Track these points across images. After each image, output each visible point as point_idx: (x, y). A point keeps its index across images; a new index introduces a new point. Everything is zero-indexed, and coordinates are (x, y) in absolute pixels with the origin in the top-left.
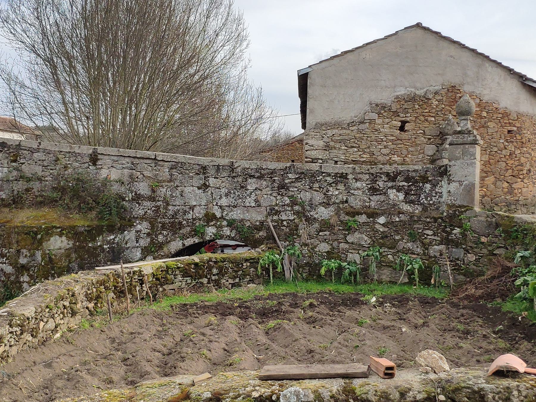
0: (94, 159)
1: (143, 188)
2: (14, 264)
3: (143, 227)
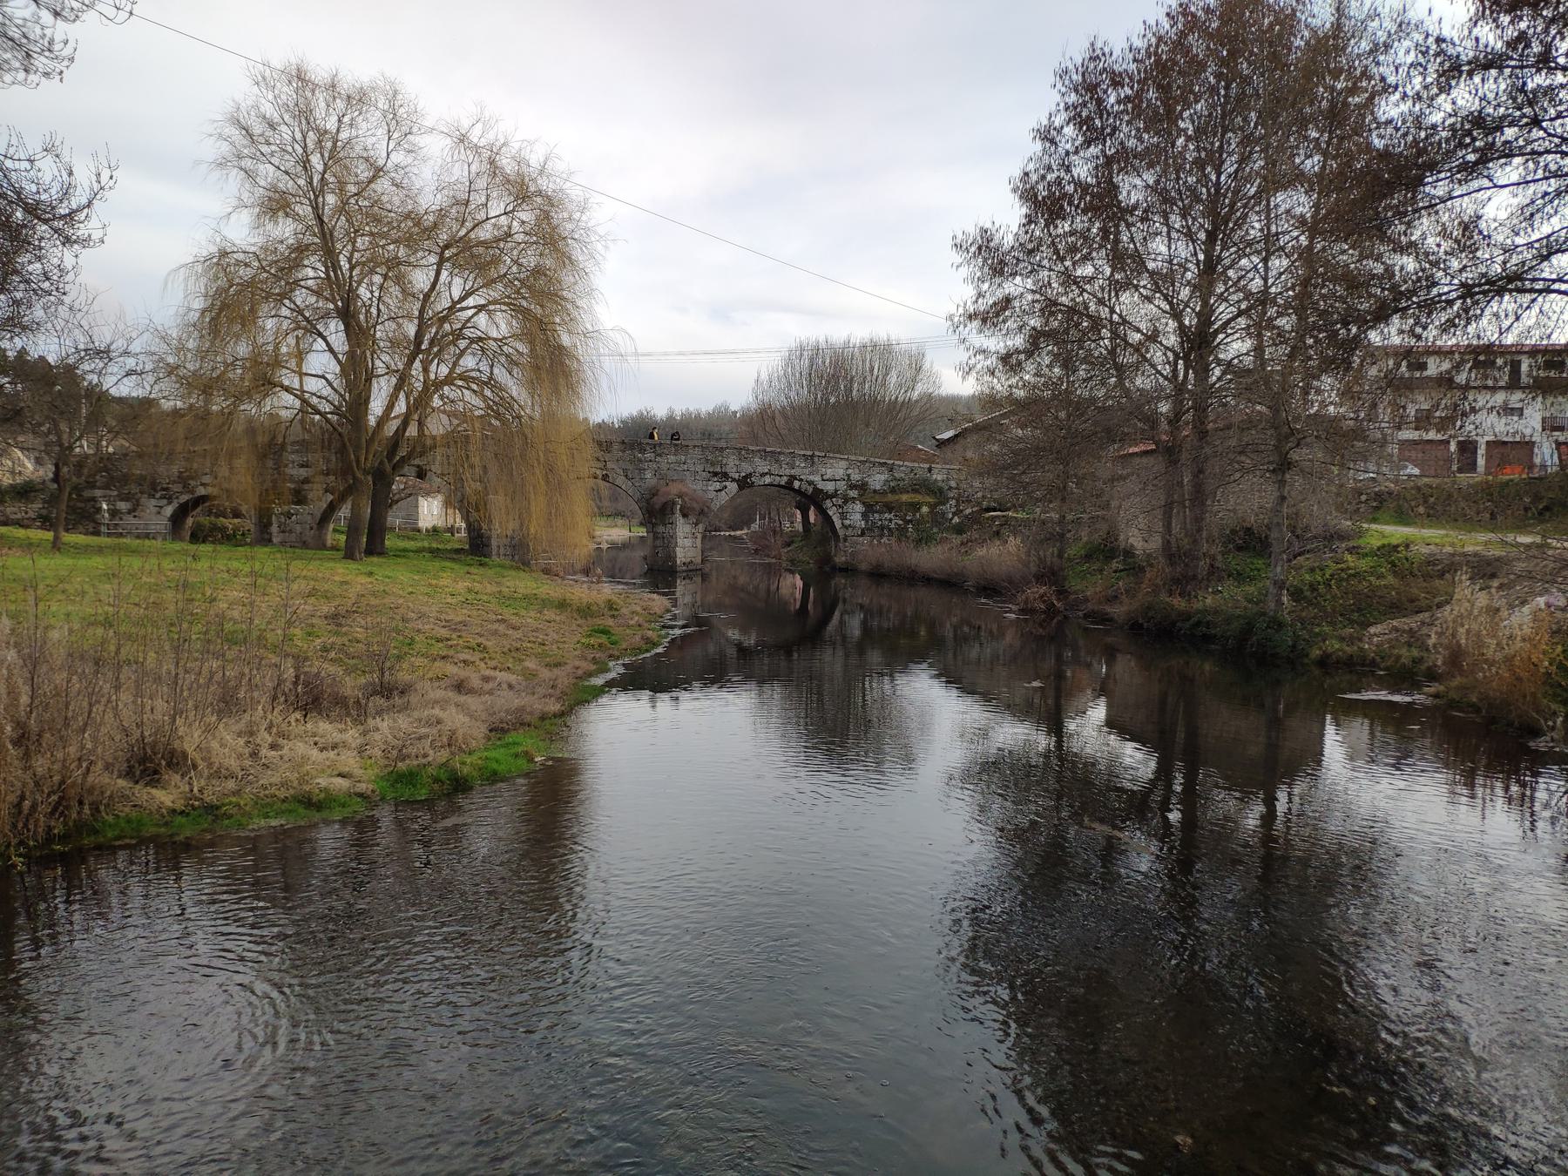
0: (930, 470)
1: (953, 484)
3: (953, 502)
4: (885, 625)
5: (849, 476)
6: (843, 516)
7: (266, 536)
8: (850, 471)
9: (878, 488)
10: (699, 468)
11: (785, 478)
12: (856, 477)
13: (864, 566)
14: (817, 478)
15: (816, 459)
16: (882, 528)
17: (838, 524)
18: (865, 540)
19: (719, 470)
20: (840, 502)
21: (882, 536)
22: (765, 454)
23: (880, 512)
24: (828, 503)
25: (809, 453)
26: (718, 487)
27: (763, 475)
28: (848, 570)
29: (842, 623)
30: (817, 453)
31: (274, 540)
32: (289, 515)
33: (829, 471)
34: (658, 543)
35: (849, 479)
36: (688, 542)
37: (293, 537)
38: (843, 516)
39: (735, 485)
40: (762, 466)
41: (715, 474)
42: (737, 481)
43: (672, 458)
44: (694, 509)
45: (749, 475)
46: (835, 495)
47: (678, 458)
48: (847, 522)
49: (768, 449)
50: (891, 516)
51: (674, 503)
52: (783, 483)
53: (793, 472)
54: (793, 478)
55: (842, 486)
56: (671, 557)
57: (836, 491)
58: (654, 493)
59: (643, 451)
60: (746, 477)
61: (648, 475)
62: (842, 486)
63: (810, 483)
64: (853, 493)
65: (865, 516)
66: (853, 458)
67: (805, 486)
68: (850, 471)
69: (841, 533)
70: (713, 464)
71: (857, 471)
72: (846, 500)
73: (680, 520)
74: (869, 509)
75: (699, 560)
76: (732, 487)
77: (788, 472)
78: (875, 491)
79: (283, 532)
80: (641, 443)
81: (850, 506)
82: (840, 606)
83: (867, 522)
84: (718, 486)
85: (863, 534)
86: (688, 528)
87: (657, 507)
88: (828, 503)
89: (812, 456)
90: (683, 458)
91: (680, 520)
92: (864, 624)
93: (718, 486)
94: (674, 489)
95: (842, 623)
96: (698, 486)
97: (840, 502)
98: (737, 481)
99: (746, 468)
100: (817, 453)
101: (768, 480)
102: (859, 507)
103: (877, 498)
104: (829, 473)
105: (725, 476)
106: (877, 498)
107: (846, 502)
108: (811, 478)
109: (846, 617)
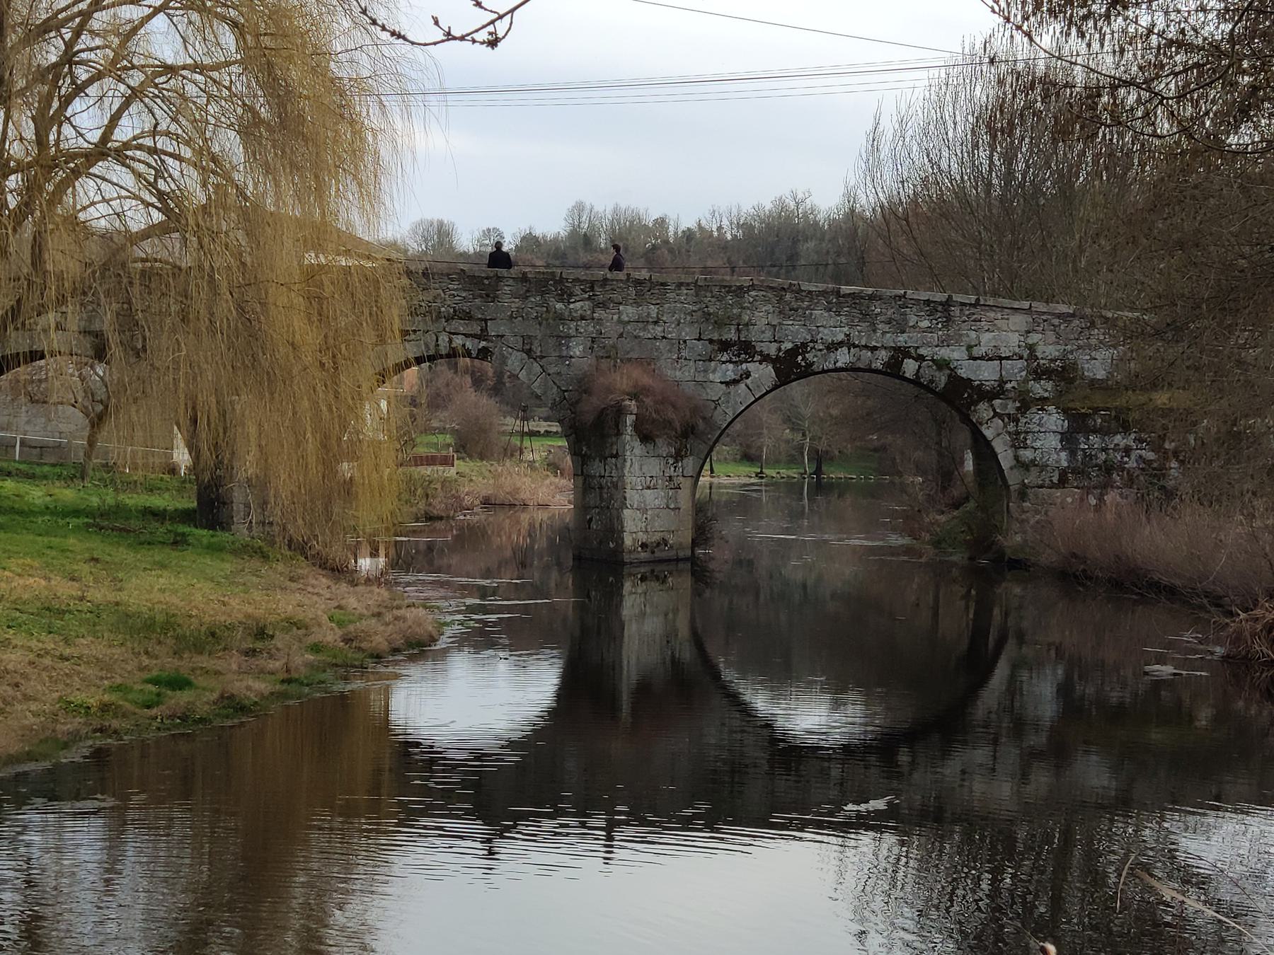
2: (1157, 447)
4: (1114, 696)
5: (1031, 348)
6: (1018, 441)
8: (1034, 338)
9: (1101, 375)
10: (688, 333)
11: (884, 355)
12: (1048, 350)
13: (1047, 558)
14: (955, 354)
15: (955, 311)
16: (1108, 468)
17: (1006, 461)
18: (1069, 496)
19: (731, 335)
20: (1011, 407)
21: (1106, 486)
22: (836, 302)
23: (1104, 432)
24: (983, 411)
25: (940, 297)
26: (730, 375)
27: (833, 347)
28: (1017, 566)
29: (1013, 688)
30: (958, 298)
33: (986, 337)
34: (593, 499)
35: (1033, 356)
36: (654, 498)
38: (1018, 441)
39: (768, 370)
40: (831, 327)
41: (725, 346)
42: (774, 361)
43: (629, 312)
44: (668, 424)
45: (801, 348)
46: (999, 391)
47: (643, 310)
48: (1027, 455)
49: (846, 289)
50: (1130, 441)
51: (620, 411)
52: (878, 365)
53: (902, 339)
54: (901, 353)
55: (1015, 370)
56: (614, 530)
57: (1002, 382)
58: (584, 386)
59: (565, 296)
60: (794, 352)
61: (577, 350)
62: (1015, 370)
63: (942, 365)
64: (1041, 388)
65: (1068, 440)
66: (1040, 306)
67: (928, 372)
68: (1034, 338)
69: (1013, 478)
70: (719, 324)
71: (1051, 336)
72: (1026, 403)
73: (633, 448)
74: (1078, 425)
75: (686, 536)
76: (763, 373)
77: (889, 340)
78: (1093, 383)
80: (562, 280)
81: (1034, 416)
82: (1010, 649)
83: (1073, 453)
84: (730, 371)
85: (1063, 482)
86: (654, 467)
87: (590, 418)
88: (983, 411)
89: (948, 304)
90: (654, 310)
91: (633, 448)
92: (1065, 691)
93: (730, 371)
94: (622, 379)
95: (1013, 688)
96: (683, 374)
97: (1011, 407)
98: (774, 361)
99: (795, 332)
100: (958, 298)
101: (843, 357)
102: (1054, 420)
103: (1098, 399)
104: (987, 341)
105: (746, 349)
106: (1098, 399)
107: (1024, 407)
108: (944, 353)
109: (1024, 675)
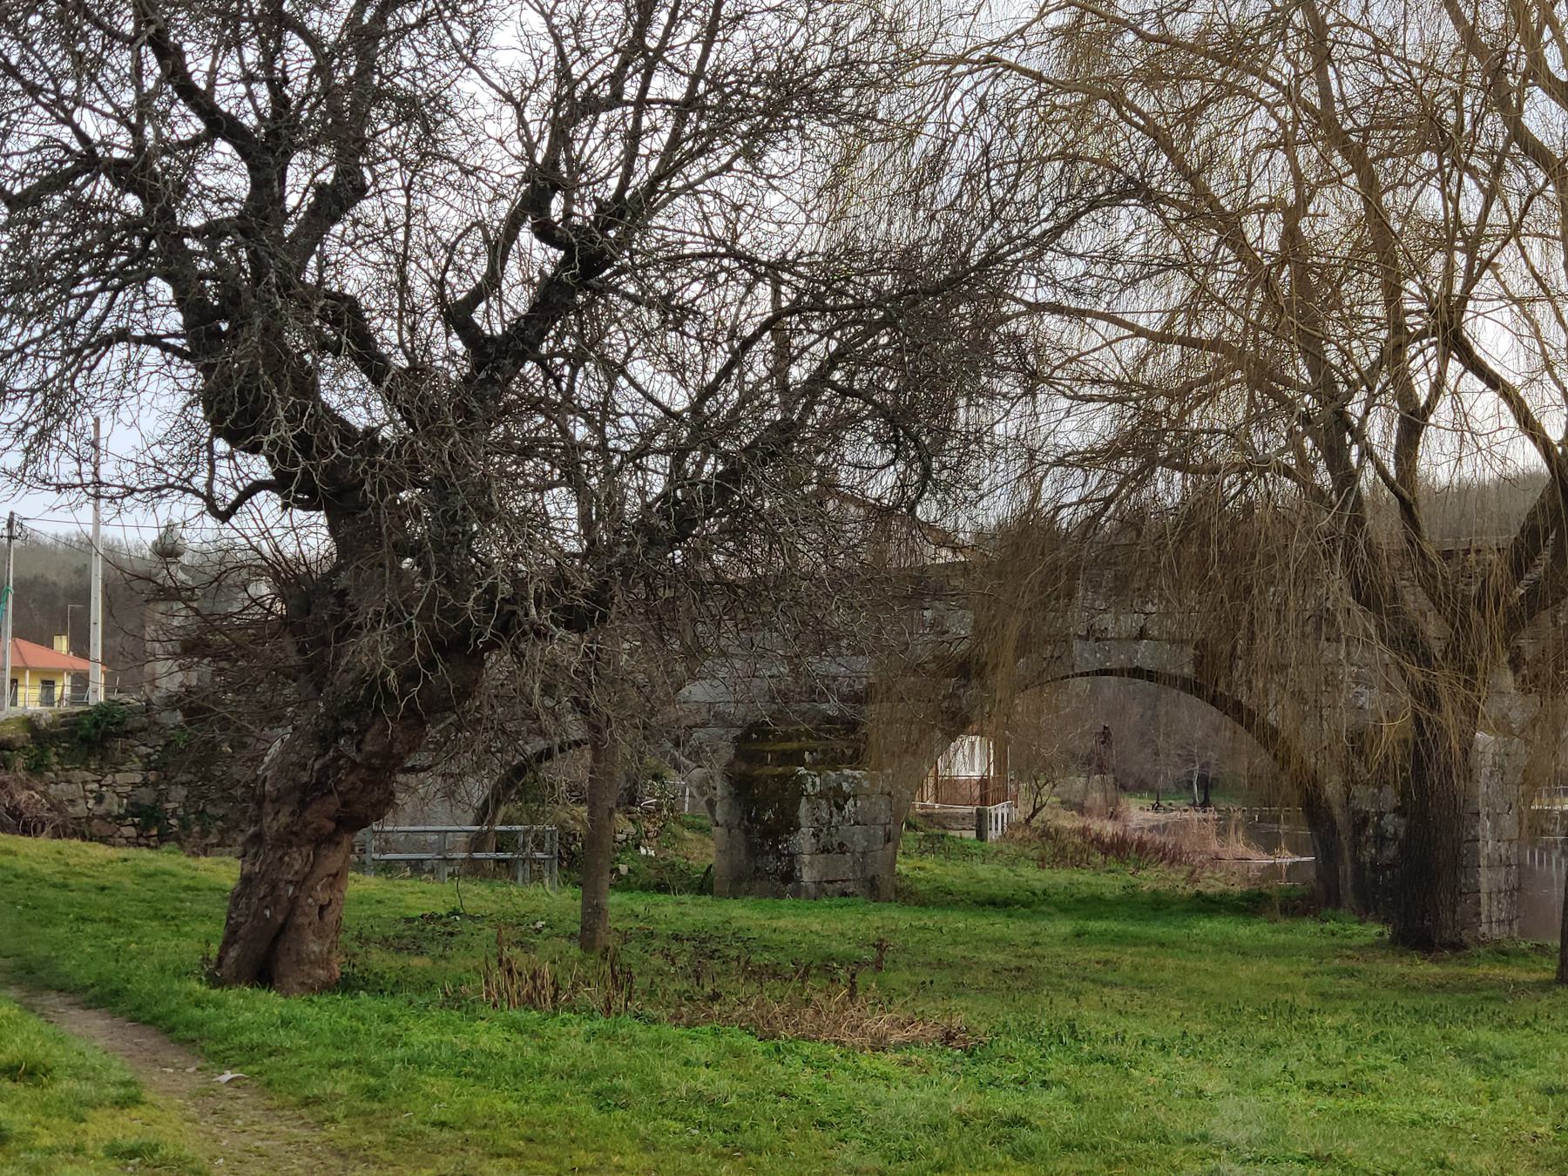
7: (772, 863)
31: (807, 876)
32: (837, 798)
37: (844, 867)
79: (825, 850)
